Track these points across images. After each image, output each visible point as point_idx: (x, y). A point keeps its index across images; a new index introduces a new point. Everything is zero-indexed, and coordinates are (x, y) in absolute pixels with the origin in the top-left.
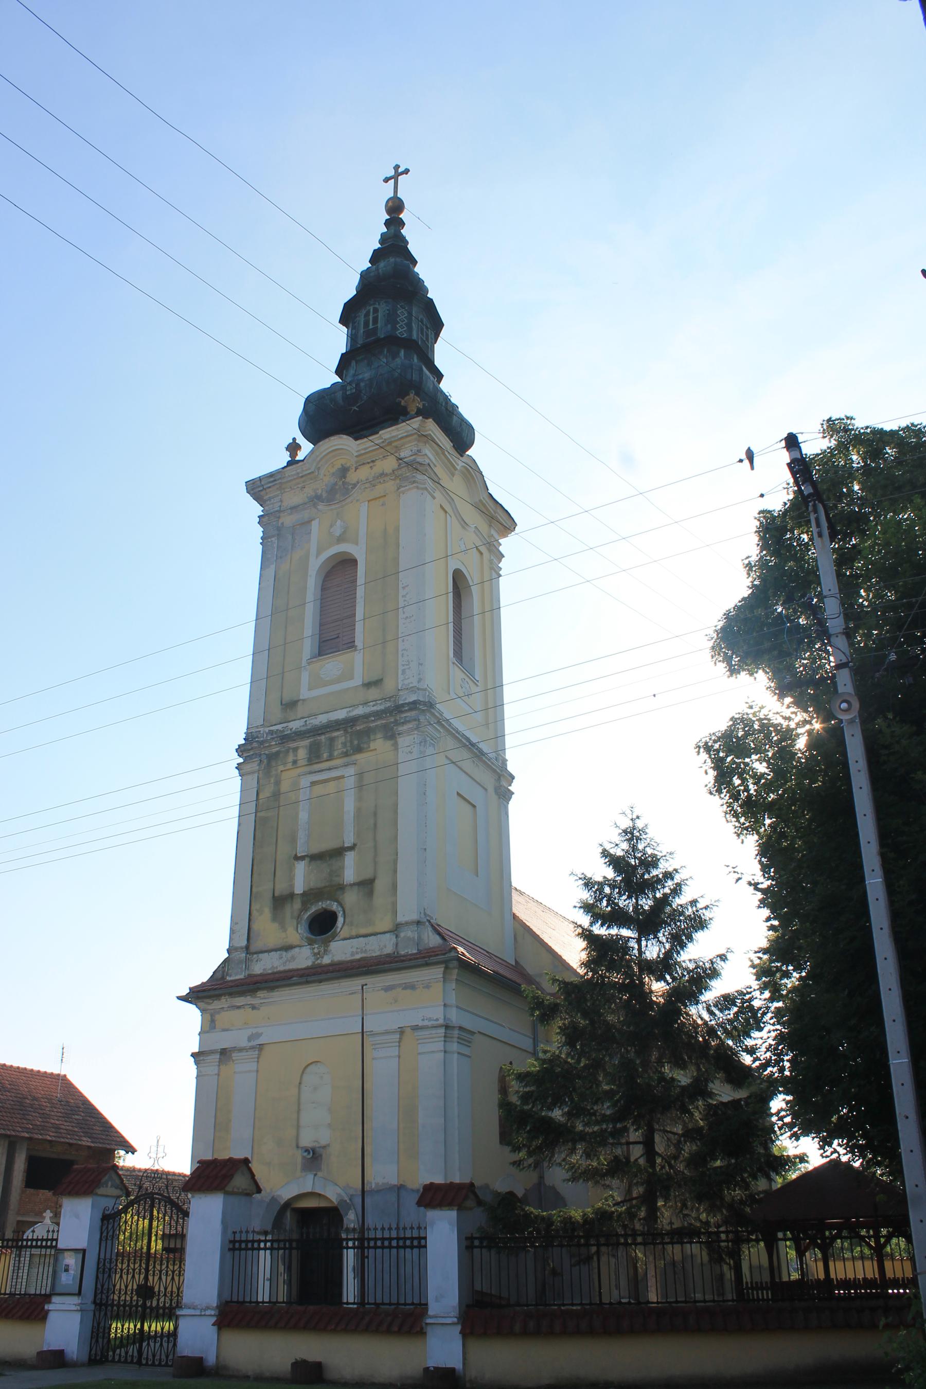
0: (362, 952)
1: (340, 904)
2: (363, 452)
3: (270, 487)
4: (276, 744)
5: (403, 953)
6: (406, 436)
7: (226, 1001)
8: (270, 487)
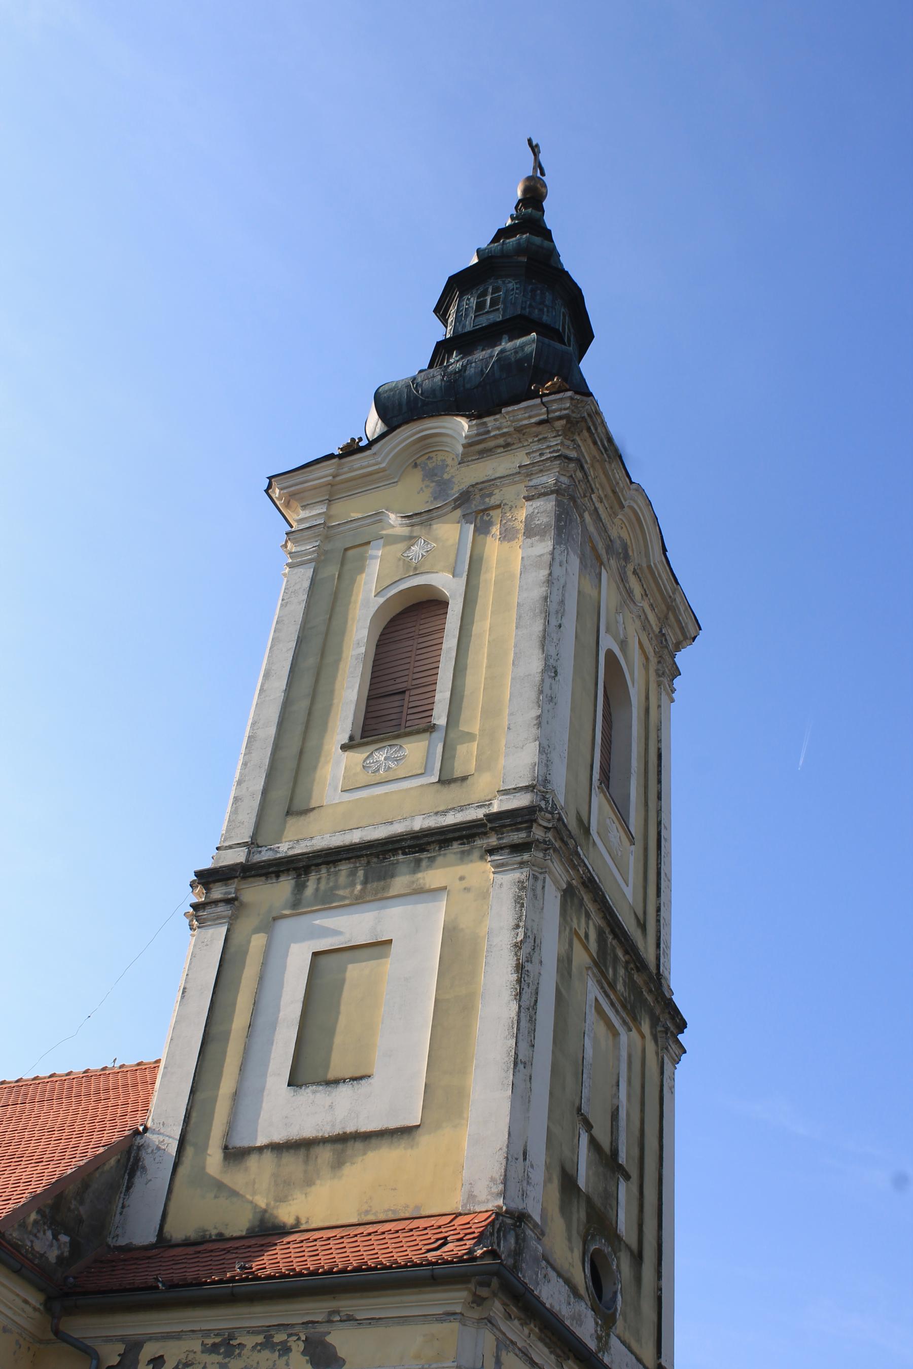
1: (618, 1266)
3: (595, 443)
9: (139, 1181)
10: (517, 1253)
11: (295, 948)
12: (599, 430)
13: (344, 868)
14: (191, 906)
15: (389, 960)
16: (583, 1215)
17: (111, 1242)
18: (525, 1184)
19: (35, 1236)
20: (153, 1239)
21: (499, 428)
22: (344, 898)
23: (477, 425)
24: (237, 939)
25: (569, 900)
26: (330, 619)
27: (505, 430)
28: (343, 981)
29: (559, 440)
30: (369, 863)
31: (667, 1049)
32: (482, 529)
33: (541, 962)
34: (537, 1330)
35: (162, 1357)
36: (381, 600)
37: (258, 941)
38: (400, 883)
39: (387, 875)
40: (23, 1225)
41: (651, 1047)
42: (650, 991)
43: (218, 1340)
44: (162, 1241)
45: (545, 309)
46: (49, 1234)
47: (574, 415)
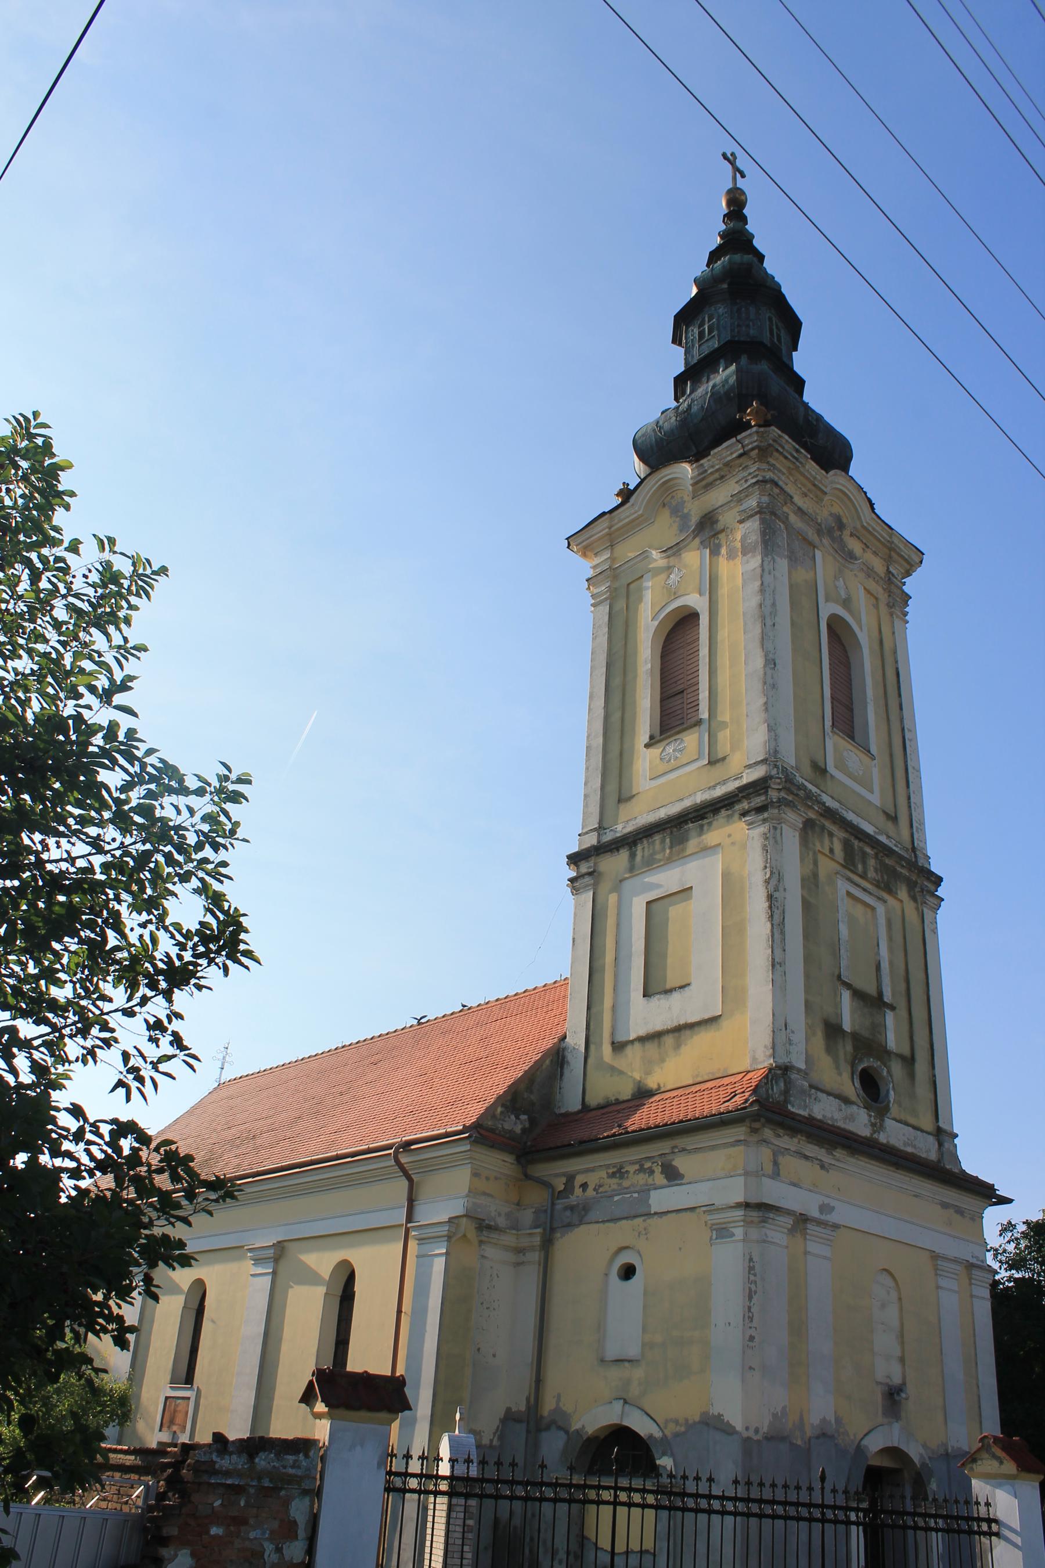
0: (914, 1147)
1: (889, 1072)
2: (870, 529)
3: (786, 458)
4: (818, 812)
5: (948, 1167)
6: (906, 560)
7: (799, 1142)
8: (786, 458)
9: (566, 1072)
10: (786, 1092)
11: (635, 900)
12: (786, 447)
13: (657, 838)
14: (569, 880)
15: (692, 901)
16: (849, 1048)
17: (557, 1111)
18: (787, 1045)
19: (504, 1121)
20: (580, 1107)
21: (713, 467)
22: (660, 860)
23: (697, 467)
24: (600, 900)
25: (810, 832)
26: (626, 644)
27: (717, 467)
28: (667, 919)
29: (757, 465)
30: (671, 832)
31: (925, 903)
32: (715, 552)
33: (785, 890)
34: (804, 1138)
35: (586, 1183)
36: (656, 623)
37: (613, 898)
38: (692, 845)
39: (683, 840)
40: (494, 1116)
41: (910, 906)
42: (903, 866)
43: (615, 1170)
44: (585, 1108)
45: (751, 323)
46: (513, 1117)
47: (762, 444)
